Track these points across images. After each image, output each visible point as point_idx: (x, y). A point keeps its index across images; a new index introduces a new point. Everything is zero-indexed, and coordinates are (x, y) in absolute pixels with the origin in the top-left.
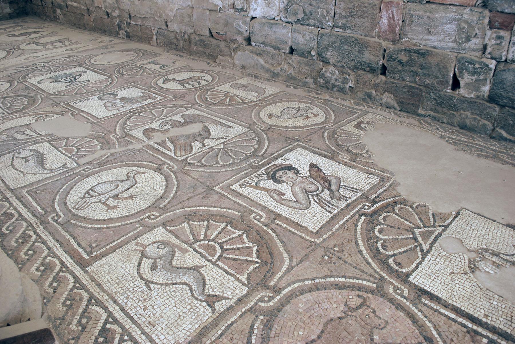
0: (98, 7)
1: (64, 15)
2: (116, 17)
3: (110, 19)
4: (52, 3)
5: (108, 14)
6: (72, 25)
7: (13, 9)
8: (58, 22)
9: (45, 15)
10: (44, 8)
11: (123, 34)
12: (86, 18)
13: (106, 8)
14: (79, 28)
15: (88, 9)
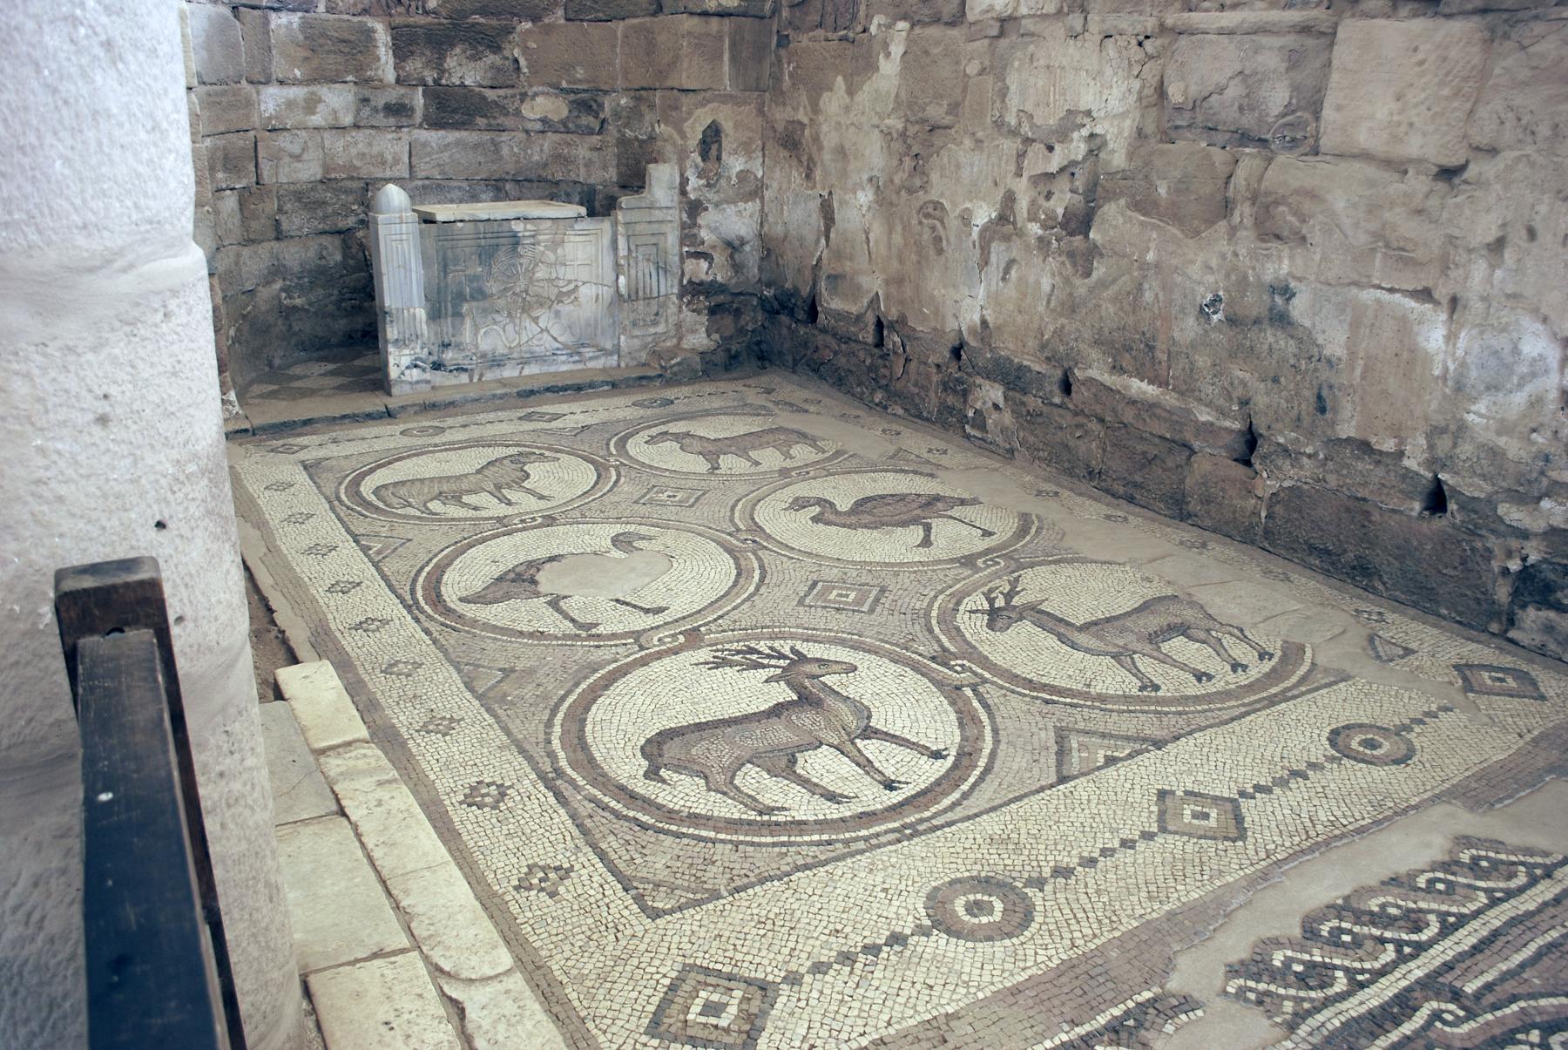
0: (1365, 447)
1: (1030, 419)
2: (1524, 535)
3: (1439, 523)
4: (957, 352)
5: (1437, 500)
6: (1070, 472)
7: (716, 336)
8: (968, 437)
9: (886, 388)
10: (885, 357)
11: (1549, 629)
12: (1202, 465)
13: (1433, 462)
14: (1131, 500)
15: (1251, 440)
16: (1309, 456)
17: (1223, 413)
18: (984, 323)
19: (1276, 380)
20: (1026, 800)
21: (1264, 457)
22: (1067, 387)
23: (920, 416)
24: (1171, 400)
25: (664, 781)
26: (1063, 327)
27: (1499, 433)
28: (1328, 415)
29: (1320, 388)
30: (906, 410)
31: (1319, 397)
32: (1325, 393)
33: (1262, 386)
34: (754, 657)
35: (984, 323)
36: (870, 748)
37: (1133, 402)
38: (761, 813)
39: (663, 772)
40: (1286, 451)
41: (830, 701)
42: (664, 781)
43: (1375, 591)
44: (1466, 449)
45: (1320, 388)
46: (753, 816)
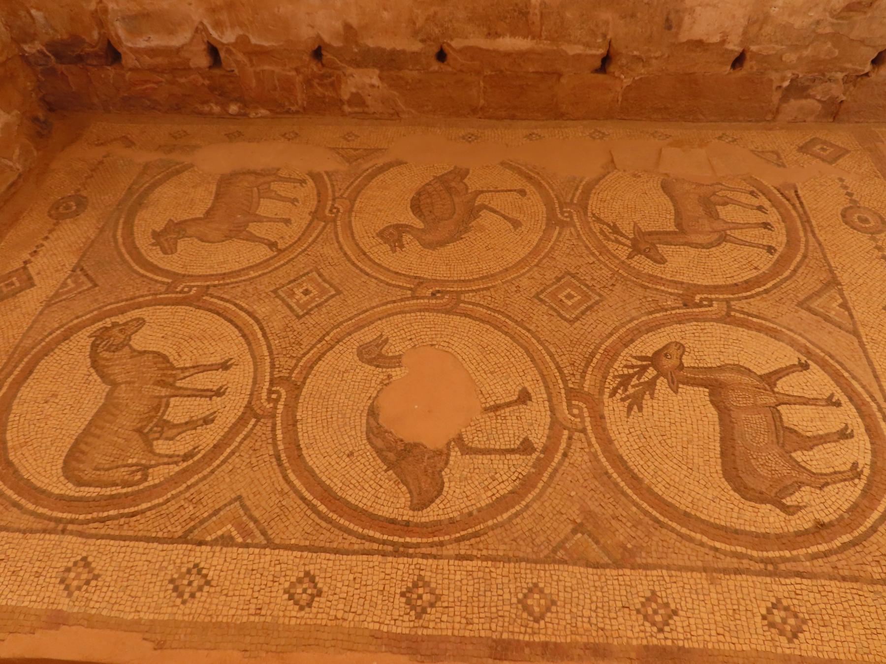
14: (513, 118)
16: (656, 58)
17: (587, 45)
18: (348, 27)
19: (633, 16)
20: (874, 360)
21: (621, 67)
22: (441, 56)
23: (288, 112)
24: (544, 45)
25: (799, 508)
26: (436, 13)
27: (790, 15)
28: (674, 30)
29: (669, 13)
30: (271, 110)
31: (667, 20)
32: (672, 16)
33: (622, 22)
34: (634, 381)
35: (348, 27)
36: (782, 385)
37: (508, 54)
38: (859, 475)
39: (788, 501)
40: (639, 59)
41: (723, 377)
42: (799, 508)
43: (699, 120)
44: (768, 29)
45: (669, 13)
46: (861, 484)
